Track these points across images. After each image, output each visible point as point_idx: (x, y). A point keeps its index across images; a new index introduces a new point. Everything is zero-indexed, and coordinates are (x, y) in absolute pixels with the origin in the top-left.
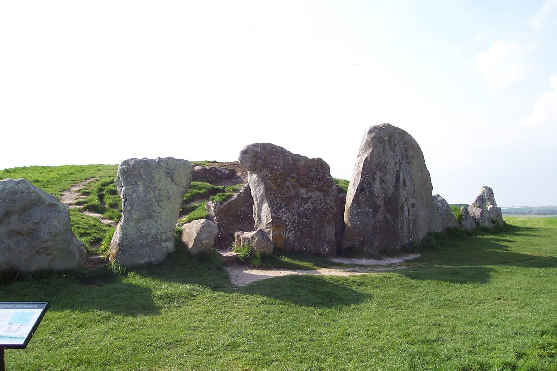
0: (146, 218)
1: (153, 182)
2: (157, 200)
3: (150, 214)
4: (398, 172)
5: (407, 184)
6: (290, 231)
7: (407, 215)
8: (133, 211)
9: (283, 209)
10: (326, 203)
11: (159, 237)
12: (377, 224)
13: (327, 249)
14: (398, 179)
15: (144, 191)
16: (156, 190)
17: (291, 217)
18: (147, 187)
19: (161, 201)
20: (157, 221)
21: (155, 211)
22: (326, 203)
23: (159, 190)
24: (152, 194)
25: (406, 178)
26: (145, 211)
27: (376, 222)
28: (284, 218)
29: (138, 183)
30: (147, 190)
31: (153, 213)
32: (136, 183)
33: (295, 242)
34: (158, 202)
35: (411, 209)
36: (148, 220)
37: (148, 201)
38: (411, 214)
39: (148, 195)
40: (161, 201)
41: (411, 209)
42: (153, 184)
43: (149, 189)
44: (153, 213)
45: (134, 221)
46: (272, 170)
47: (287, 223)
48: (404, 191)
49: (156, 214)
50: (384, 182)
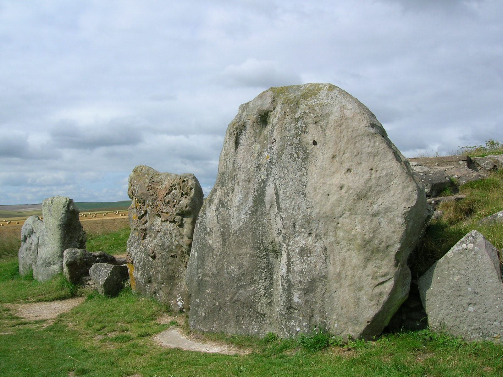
4: (264, 182)
5: (282, 206)
7: (284, 270)
11: (47, 260)
12: (207, 279)
13: (179, 303)
14: (259, 199)
17: (139, 253)
25: (281, 195)
27: (204, 275)
33: (145, 285)
35: (296, 259)
38: (296, 268)
41: (296, 259)
48: (278, 219)
50: (223, 206)
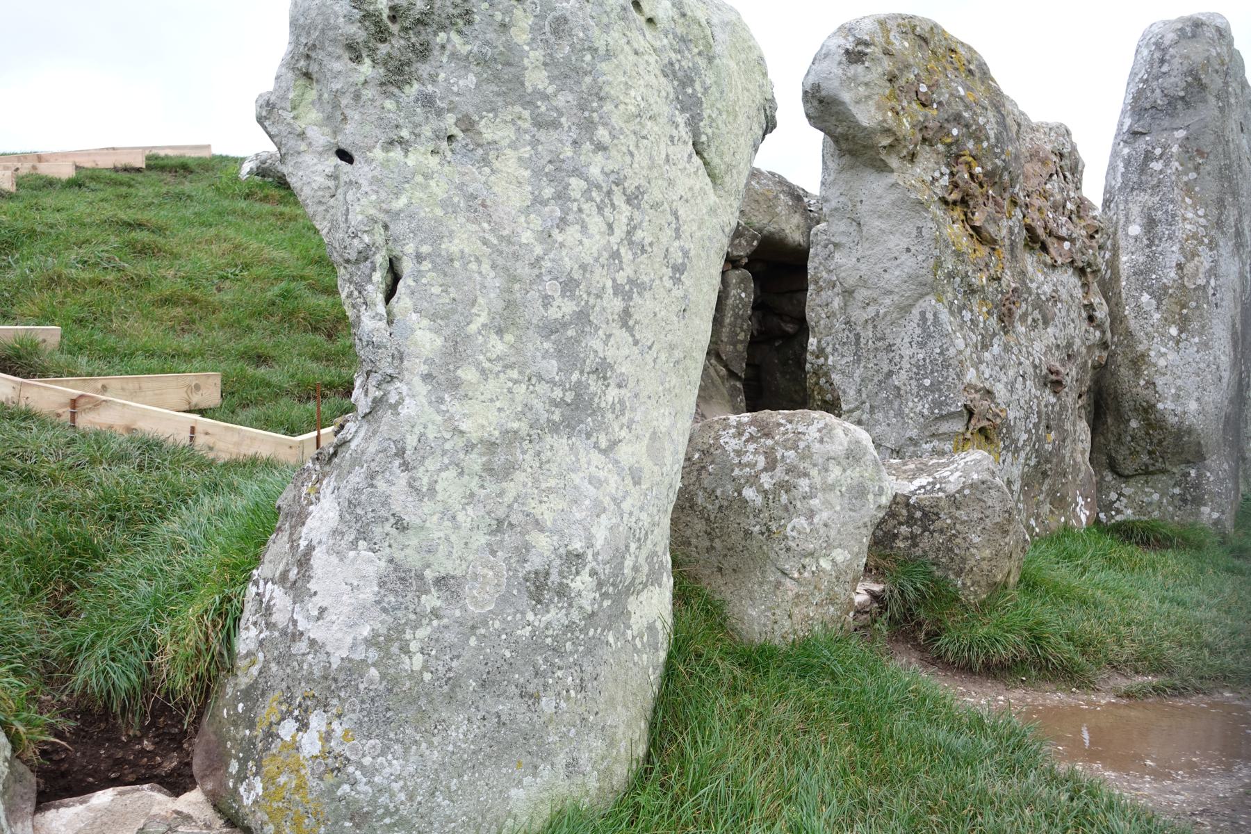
0: (554, 428)
1: (602, 134)
2: (621, 277)
3: (579, 388)
6: (1017, 451)
8: (468, 374)
9: (996, 349)
10: (1091, 319)
15: (538, 201)
16: (619, 199)
18: (557, 171)
19: (642, 288)
20: (614, 444)
21: (602, 370)
22: (1091, 319)
23: (633, 199)
24: (596, 223)
26: (551, 367)
28: (1000, 390)
29: (488, 131)
30: (562, 196)
31: (594, 385)
32: (468, 125)
34: (628, 297)
36: (560, 443)
37: (569, 286)
39: (573, 233)
40: (642, 288)
42: (600, 147)
43: (576, 184)
44: (594, 385)
45: (475, 461)
46: (954, 157)
47: (1011, 415)
49: (613, 393)
